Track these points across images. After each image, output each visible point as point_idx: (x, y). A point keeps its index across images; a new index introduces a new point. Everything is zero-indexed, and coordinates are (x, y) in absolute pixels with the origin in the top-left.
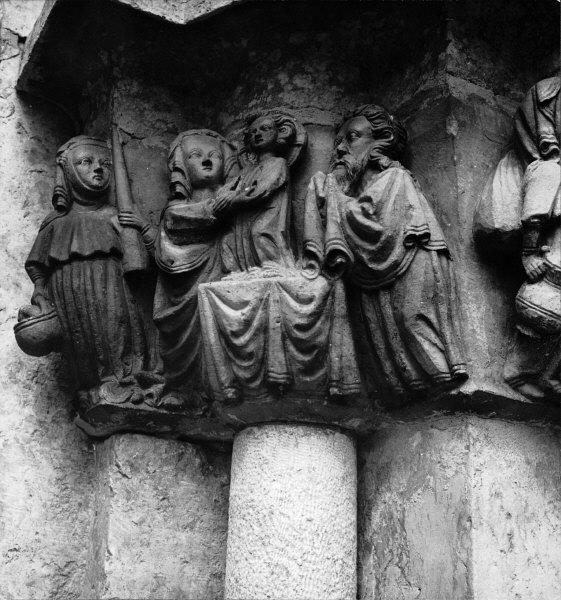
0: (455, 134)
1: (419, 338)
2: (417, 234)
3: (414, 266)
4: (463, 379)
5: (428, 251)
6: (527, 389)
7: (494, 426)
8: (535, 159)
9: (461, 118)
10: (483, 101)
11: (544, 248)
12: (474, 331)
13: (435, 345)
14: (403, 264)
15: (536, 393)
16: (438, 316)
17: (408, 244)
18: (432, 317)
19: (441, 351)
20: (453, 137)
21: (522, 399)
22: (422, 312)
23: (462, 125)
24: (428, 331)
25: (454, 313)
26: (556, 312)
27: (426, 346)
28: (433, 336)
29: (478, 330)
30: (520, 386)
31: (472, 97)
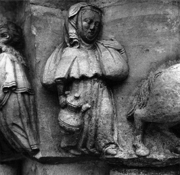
0: (35, 33)
1: (15, 133)
2: (8, 87)
3: (9, 101)
4: (37, 151)
5: (17, 93)
6: (72, 151)
7: (61, 166)
8: (68, 46)
9: (38, 26)
10: (53, 15)
11: (66, 92)
12: (43, 128)
13: (23, 136)
14: (3, 101)
15: (77, 153)
16: (23, 123)
17: (5, 91)
18: (20, 124)
19: (26, 138)
20: (34, 36)
21: (70, 156)
22: (14, 122)
23: (38, 29)
24: (19, 130)
25: (32, 120)
26: (71, 124)
27: (19, 137)
28: (21, 132)
29: (46, 127)
30: (69, 150)
31: (46, 14)
